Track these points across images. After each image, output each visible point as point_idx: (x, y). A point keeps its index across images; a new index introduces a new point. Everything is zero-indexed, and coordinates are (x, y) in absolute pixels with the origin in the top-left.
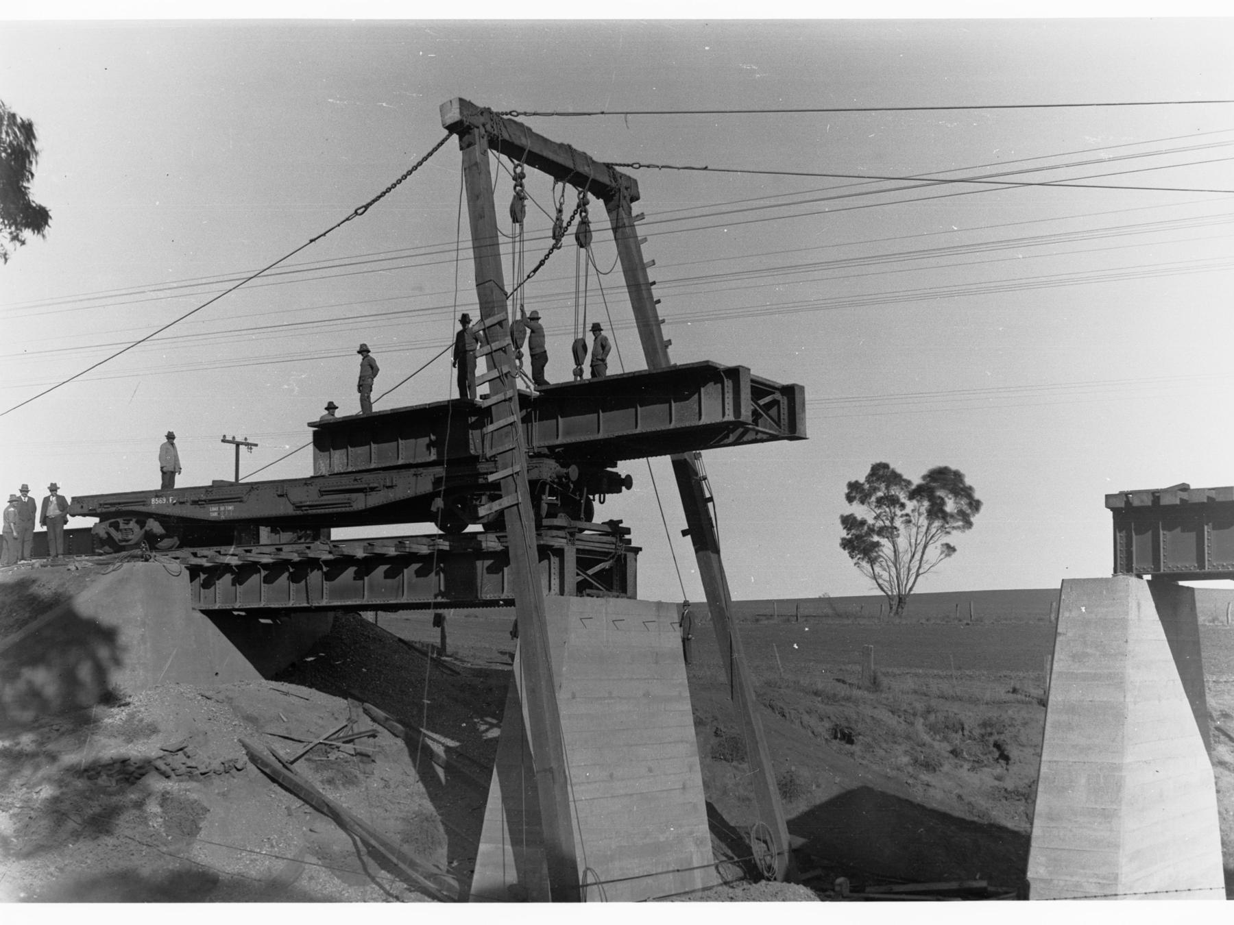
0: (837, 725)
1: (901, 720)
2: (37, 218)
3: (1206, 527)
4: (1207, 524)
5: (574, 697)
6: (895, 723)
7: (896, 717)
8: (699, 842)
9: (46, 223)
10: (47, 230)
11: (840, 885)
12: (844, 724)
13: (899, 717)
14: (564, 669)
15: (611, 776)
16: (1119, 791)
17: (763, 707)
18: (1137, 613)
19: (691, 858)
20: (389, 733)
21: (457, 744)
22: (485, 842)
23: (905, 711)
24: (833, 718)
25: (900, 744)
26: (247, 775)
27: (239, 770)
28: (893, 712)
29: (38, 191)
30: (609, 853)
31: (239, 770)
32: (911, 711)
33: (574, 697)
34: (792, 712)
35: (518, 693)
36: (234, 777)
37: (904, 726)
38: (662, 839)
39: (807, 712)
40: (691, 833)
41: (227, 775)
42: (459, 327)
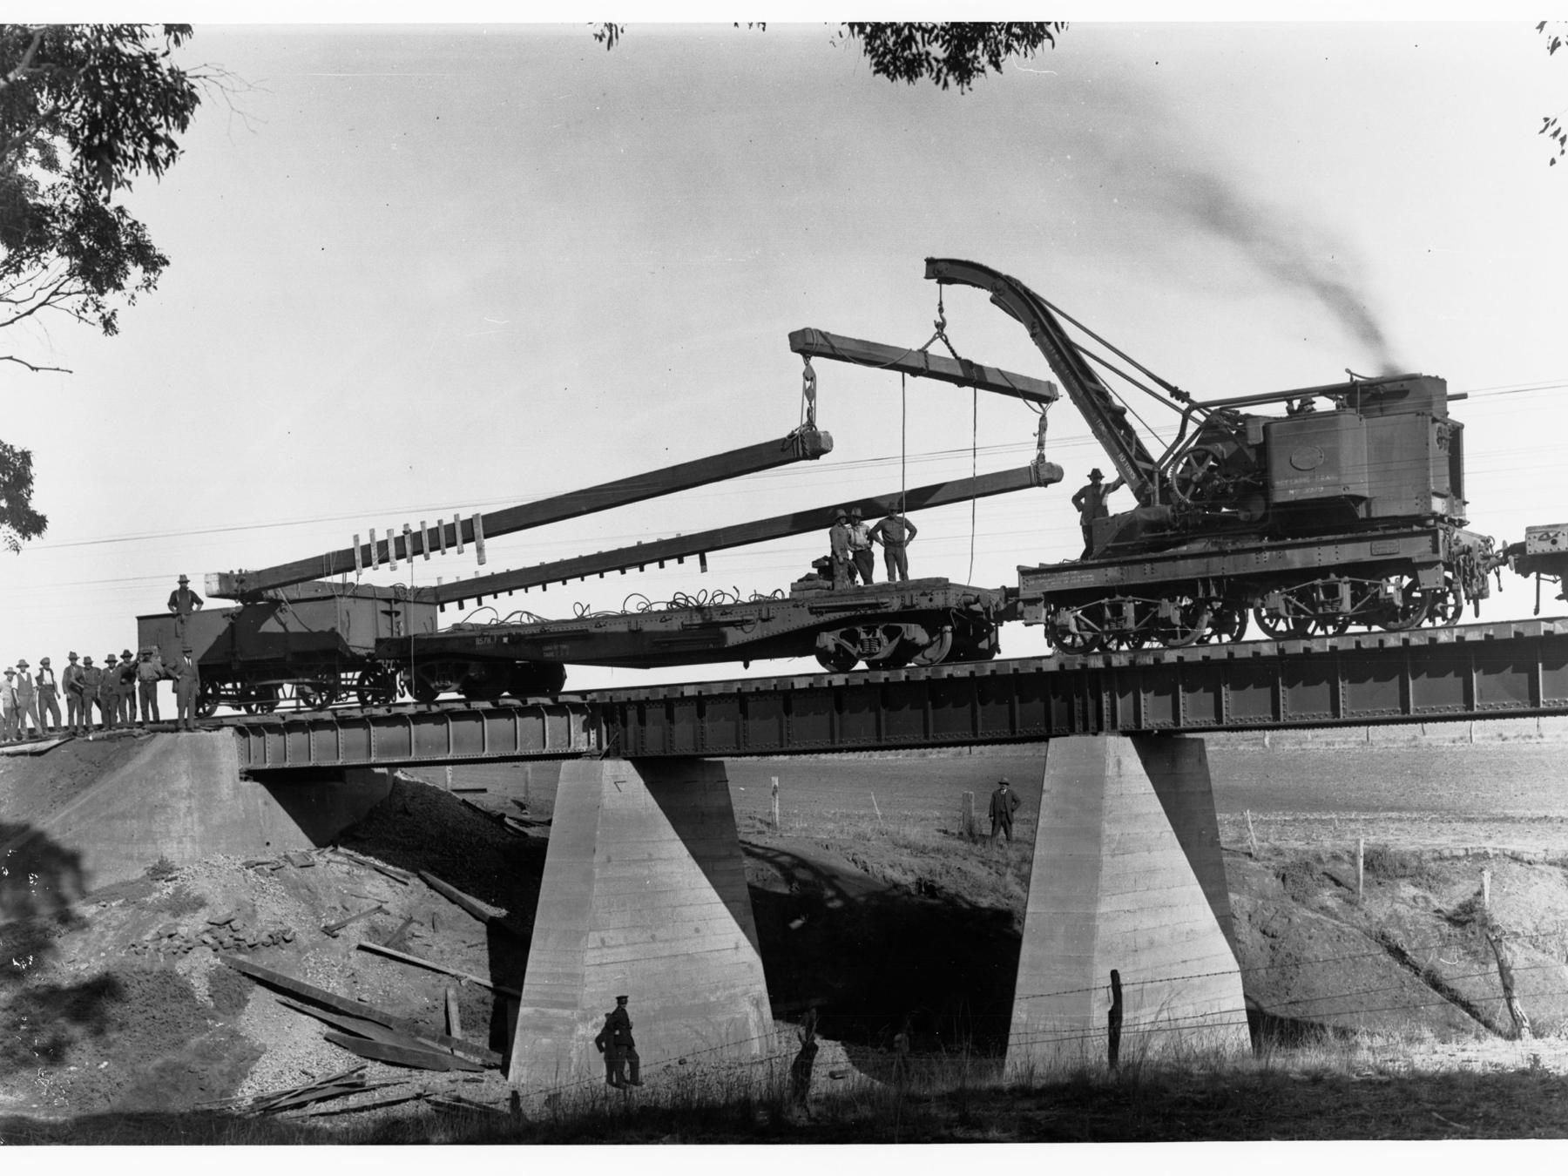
0: (920, 879)
1: (992, 871)
2: (32, 524)
3: (1223, 689)
4: (1225, 685)
5: (609, 860)
6: (985, 874)
7: (987, 868)
8: (757, 1004)
9: (45, 526)
10: (43, 533)
11: (899, 1042)
12: (928, 877)
13: (991, 868)
14: (598, 833)
15: (653, 937)
16: (1092, 939)
17: (845, 860)
18: (1116, 769)
19: (747, 1019)
20: (446, 900)
21: (504, 912)
22: (525, 1006)
23: (997, 862)
24: (917, 871)
25: (985, 897)
26: (296, 947)
27: (287, 941)
28: (984, 864)
29: (38, 503)
30: (652, 1014)
31: (287, 941)
32: (1004, 862)
33: (609, 860)
34: (875, 865)
35: (432, 870)
36: (283, 949)
37: (994, 877)
38: (712, 999)
39: (891, 866)
40: (746, 993)
41: (276, 947)
42: (68, 663)
